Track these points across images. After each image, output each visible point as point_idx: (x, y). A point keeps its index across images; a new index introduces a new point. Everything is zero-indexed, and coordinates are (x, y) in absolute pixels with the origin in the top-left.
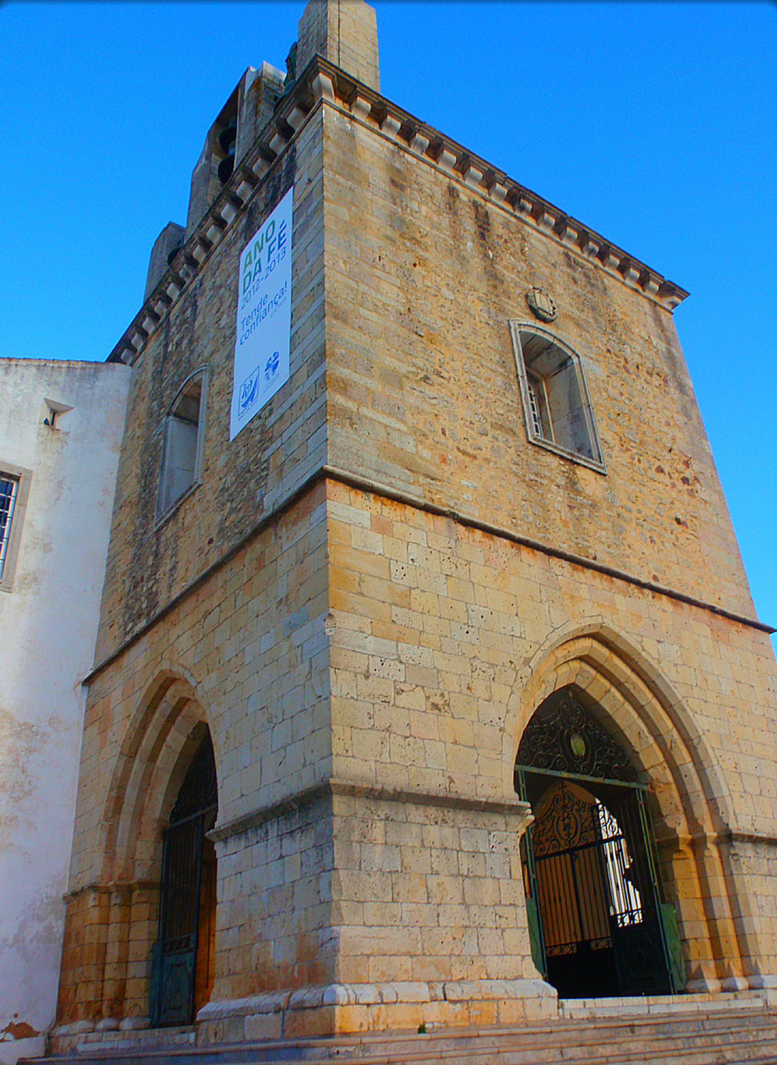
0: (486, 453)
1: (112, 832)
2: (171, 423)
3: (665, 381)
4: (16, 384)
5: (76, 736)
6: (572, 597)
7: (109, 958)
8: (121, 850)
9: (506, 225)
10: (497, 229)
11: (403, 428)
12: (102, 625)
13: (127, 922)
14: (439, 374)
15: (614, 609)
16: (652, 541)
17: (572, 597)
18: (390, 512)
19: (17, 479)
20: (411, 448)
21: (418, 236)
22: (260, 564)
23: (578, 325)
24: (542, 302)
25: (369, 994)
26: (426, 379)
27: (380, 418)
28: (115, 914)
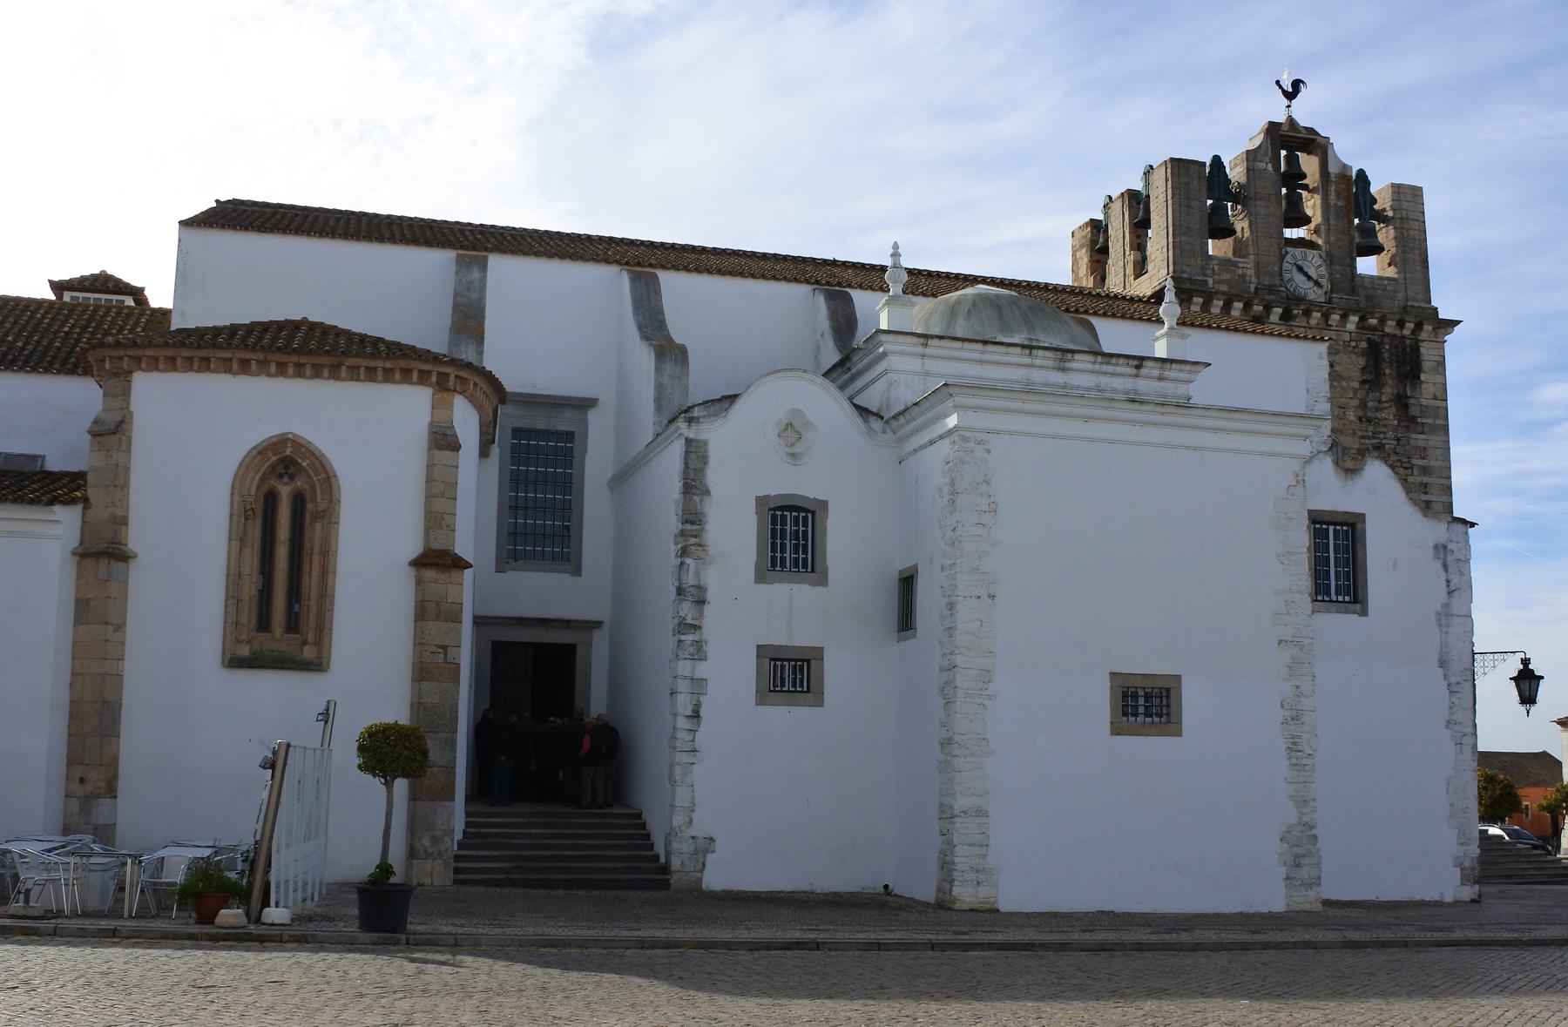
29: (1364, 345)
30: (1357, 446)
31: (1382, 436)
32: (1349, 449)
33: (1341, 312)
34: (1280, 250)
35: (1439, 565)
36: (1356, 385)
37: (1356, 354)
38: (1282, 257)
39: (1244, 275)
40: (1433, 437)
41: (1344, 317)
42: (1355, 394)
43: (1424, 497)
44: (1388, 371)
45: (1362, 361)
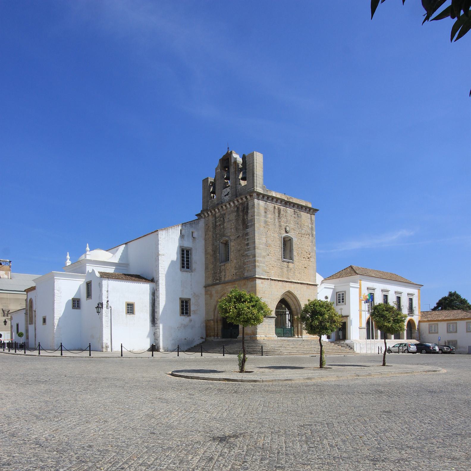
0: (276, 266)
1: (214, 312)
2: (220, 244)
3: (309, 235)
4: (187, 229)
5: (204, 296)
6: (285, 287)
7: (215, 329)
8: (216, 315)
9: (283, 211)
10: (282, 212)
11: (265, 265)
12: (206, 277)
13: (218, 325)
14: (270, 253)
15: (291, 287)
16: (300, 273)
17: (285, 287)
18: (263, 281)
19: (190, 250)
20: (266, 269)
21: (269, 224)
22: (245, 284)
23: (294, 230)
24: (288, 229)
25: (260, 336)
26: (268, 255)
27: (262, 265)
28: (216, 324)
29: (236, 209)
30: (234, 238)
31: (239, 233)
32: (232, 240)
33: (228, 203)
34: (221, 191)
35: (99, 287)
36: (233, 221)
37: (234, 212)
38: (222, 193)
39: (215, 203)
40: (251, 228)
41: (230, 204)
42: (233, 223)
43: (248, 247)
44: (241, 214)
45: (235, 214)
